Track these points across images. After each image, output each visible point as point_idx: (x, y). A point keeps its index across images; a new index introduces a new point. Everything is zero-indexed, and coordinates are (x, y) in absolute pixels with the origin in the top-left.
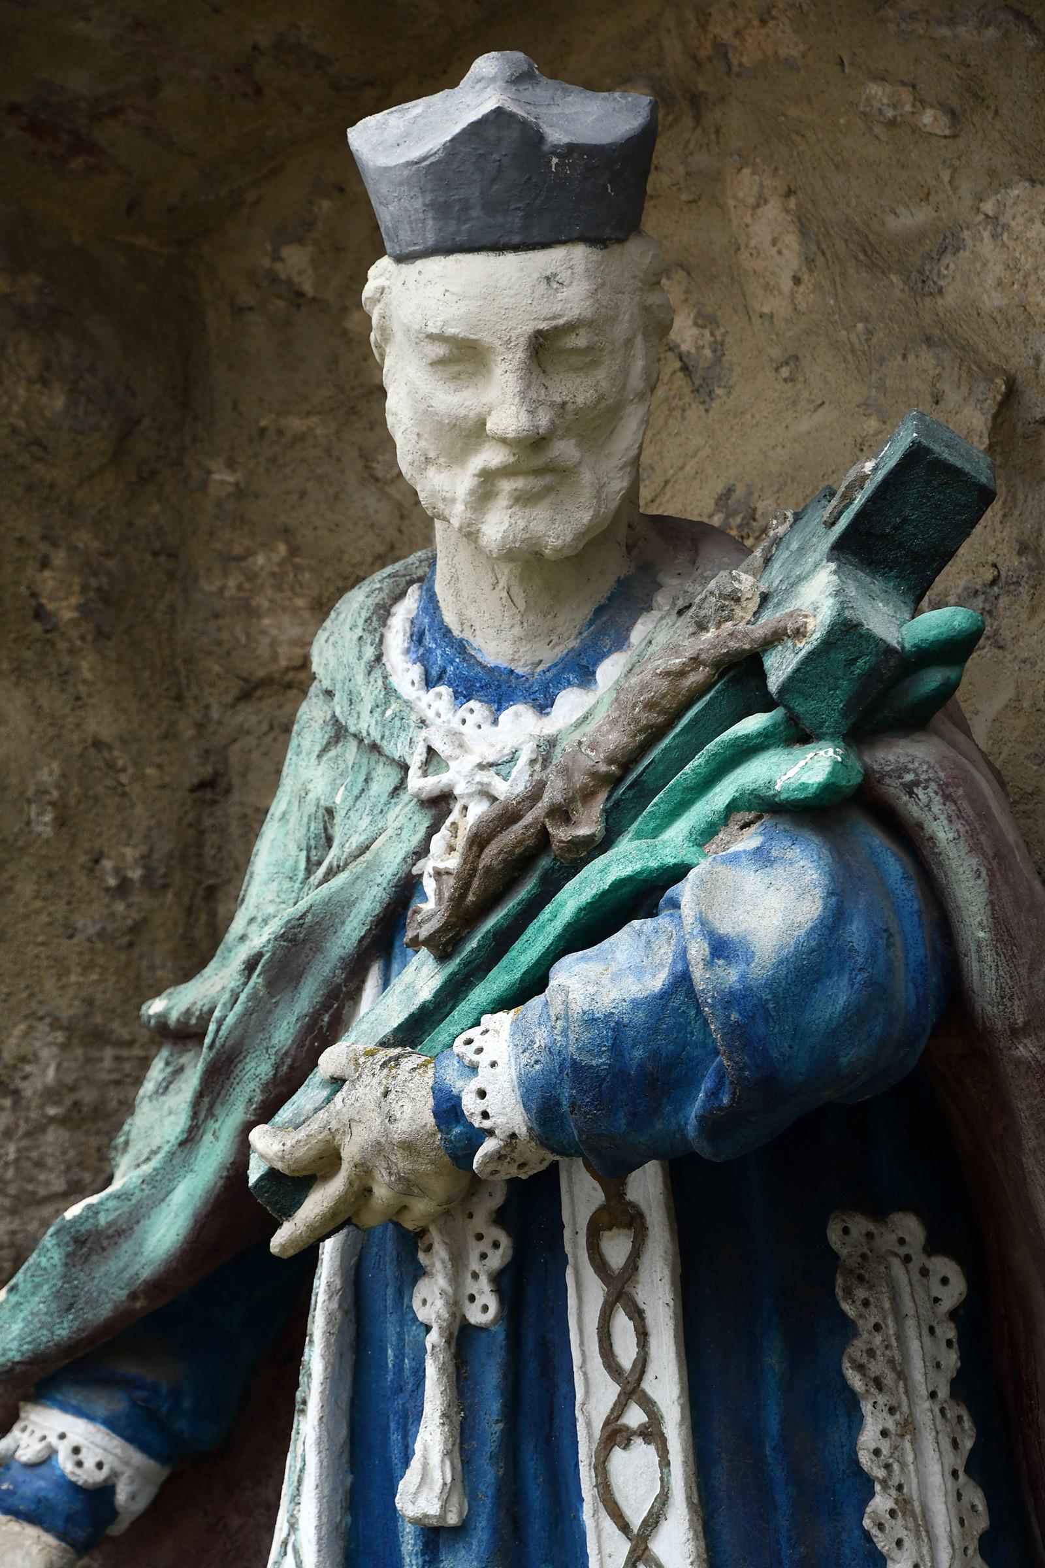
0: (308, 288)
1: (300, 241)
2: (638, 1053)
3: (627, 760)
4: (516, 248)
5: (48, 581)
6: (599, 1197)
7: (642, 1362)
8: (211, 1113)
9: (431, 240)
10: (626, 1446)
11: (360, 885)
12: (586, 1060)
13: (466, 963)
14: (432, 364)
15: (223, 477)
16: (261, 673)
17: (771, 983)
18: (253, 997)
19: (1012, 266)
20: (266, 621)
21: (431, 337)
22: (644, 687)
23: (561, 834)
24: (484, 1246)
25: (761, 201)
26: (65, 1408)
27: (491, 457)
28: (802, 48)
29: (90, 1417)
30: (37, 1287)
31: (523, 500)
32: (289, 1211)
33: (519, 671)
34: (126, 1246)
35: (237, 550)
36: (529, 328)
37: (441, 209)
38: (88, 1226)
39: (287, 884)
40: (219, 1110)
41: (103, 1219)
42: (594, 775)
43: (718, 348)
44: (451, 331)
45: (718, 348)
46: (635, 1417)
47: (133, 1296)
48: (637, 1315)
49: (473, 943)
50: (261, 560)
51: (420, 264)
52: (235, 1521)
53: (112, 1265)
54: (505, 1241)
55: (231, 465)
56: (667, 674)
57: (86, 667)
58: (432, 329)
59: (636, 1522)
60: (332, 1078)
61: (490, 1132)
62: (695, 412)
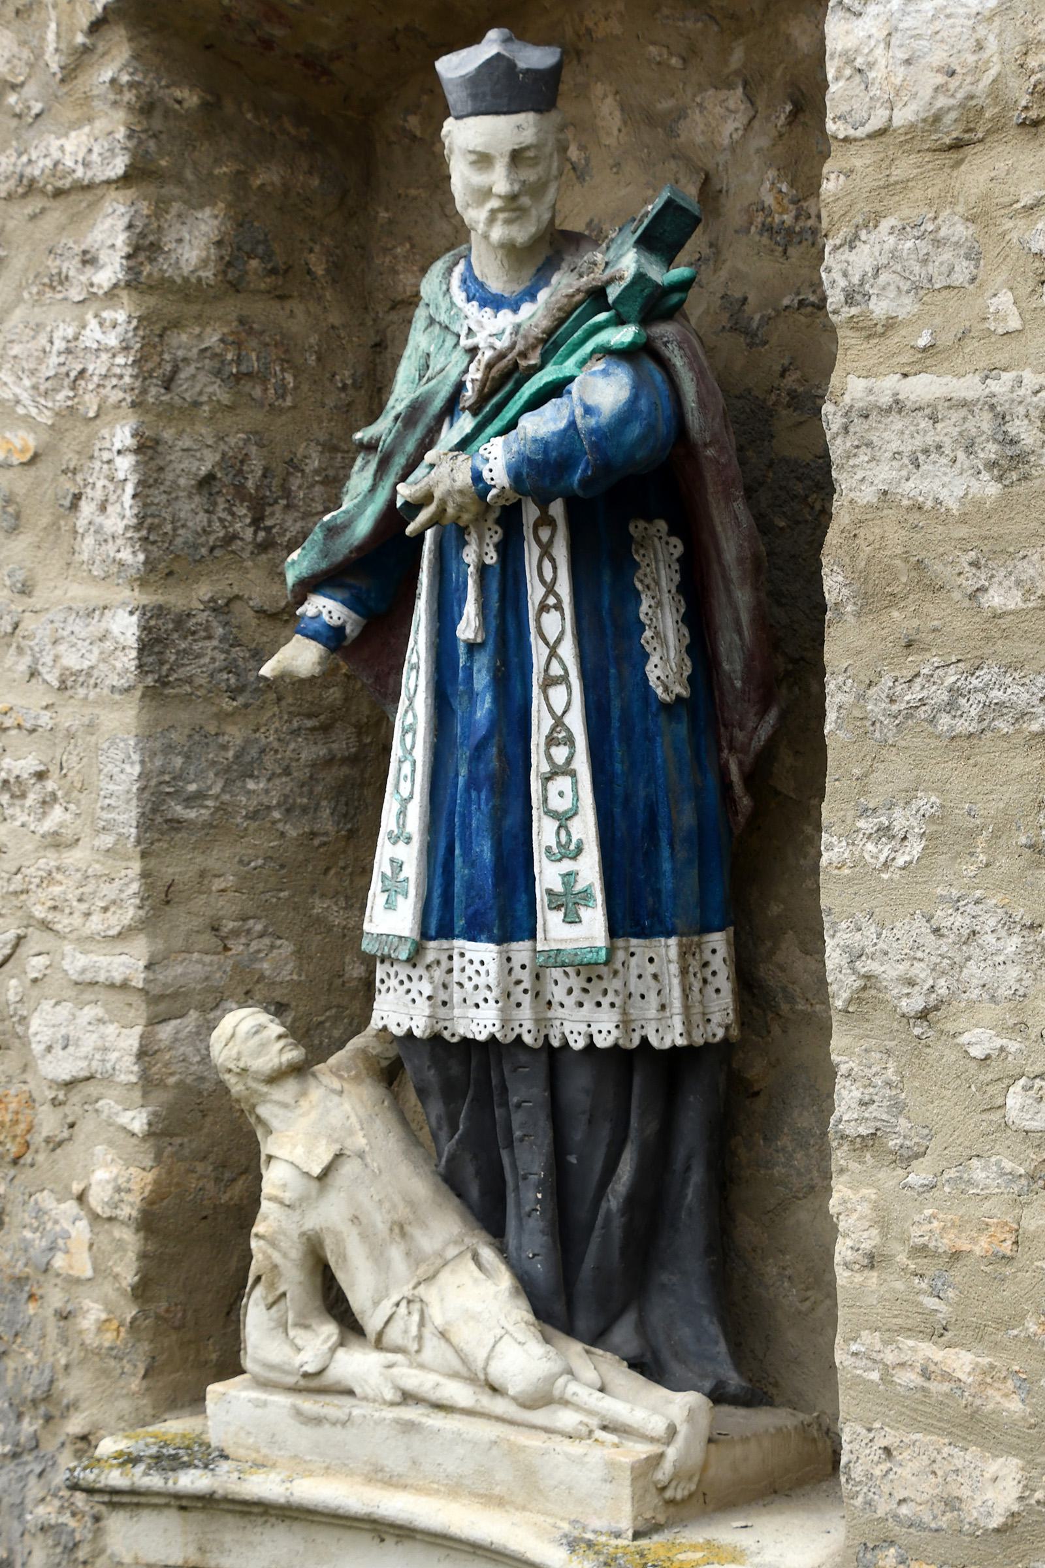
0: (418, 133)
1: (415, 114)
2: (554, 454)
3: (550, 332)
4: (505, 113)
5: (312, 258)
6: (538, 513)
7: (555, 579)
8: (381, 479)
9: (469, 109)
10: (548, 612)
12: (533, 457)
13: (484, 417)
15: (384, 215)
16: (399, 298)
17: (608, 425)
18: (397, 431)
19: (708, 125)
20: (401, 276)
21: (470, 152)
22: (557, 302)
23: (523, 363)
24: (492, 533)
25: (605, 96)
26: (325, 596)
27: (495, 203)
29: (335, 600)
31: (508, 222)
32: (413, 518)
33: (506, 295)
34: (348, 532)
35: (389, 246)
36: (510, 147)
37: (474, 96)
40: (384, 478)
41: (339, 521)
42: (537, 338)
43: (587, 160)
44: (479, 149)
45: (587, 160)
46: (552, 601)
47: (351, 552)
48: (553, 561)
49: (487, 409)
50: (399, 250)
51: (465, 120)
52: (393, 641)
54: (500, 531)
55: (387, 210)
56: (567, 296)
57: (328, 295)
59: (551, 642)
61: (494, 486)
62: (577, 187)
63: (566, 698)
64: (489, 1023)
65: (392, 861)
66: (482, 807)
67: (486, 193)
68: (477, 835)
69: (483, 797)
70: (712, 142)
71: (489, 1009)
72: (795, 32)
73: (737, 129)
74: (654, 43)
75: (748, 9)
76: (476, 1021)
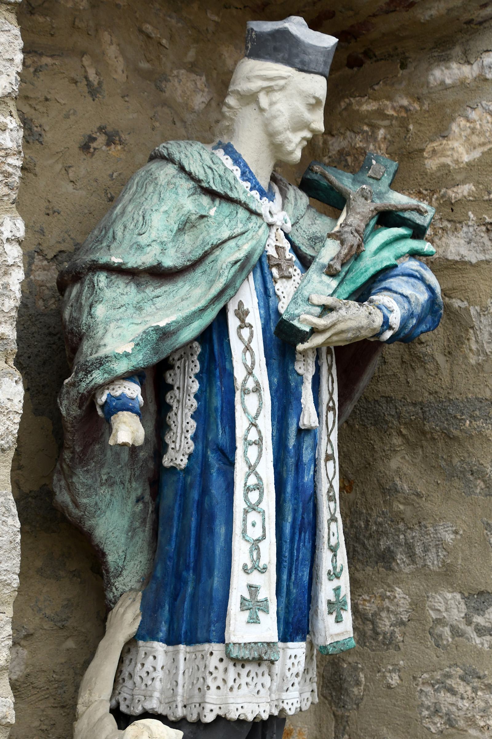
11: (258, 245)
14: (307, 104)
19: (184, 92)
25: (112, 44)
28: (125, 4)
30: (146, 345)
38: (168, 330)
39: (170, 233)
40: (216, 303)
41: (172, 328)
45: (100, 83)
51: (312, 75)
53: (169, 342)
58: (317, 95)
60: (323, 305)
63: (333, 470)
64: (295, 701)
65: (250, 587)
66: (306, 544)
67: (306, 126)
68: (301, 564)
69: (307, 537)
70: (187, 104)
71: (295, 691)
72: (226, 55)
73: (203, 102)
74: (149, 23)
75: (205, 28)
76: (285, 702)
